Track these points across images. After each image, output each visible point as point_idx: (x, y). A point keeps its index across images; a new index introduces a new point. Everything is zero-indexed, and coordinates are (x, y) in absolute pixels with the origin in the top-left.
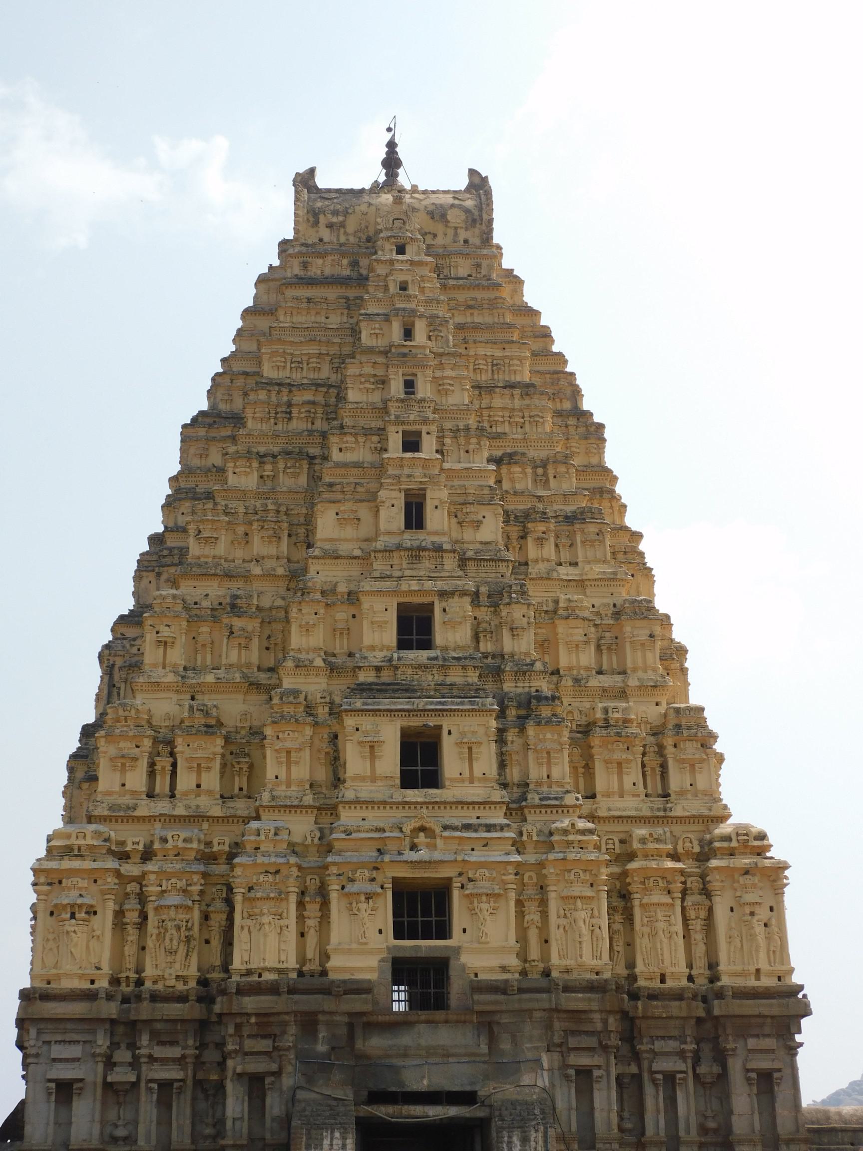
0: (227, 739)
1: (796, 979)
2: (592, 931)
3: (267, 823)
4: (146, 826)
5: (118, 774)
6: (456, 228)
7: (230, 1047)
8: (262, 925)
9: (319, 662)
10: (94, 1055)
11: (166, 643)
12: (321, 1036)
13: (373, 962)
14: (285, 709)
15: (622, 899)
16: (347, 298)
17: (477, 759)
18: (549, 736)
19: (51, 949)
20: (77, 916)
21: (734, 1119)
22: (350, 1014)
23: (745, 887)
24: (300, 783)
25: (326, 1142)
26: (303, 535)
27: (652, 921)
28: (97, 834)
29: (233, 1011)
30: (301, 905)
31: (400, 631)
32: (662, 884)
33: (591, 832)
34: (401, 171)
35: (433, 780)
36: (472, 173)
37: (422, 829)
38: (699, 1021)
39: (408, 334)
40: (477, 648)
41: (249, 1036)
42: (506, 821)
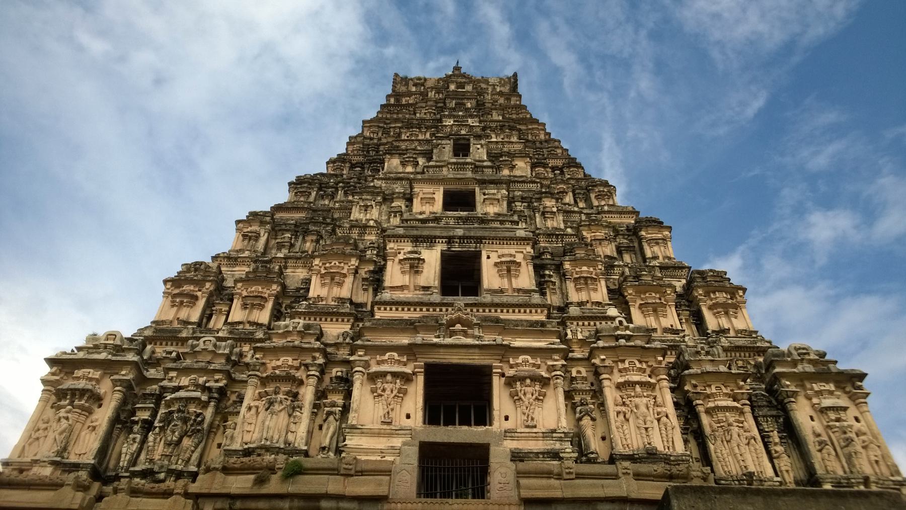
6: (494, 85)
8: (271, 403)
13: (397, 442)
17: (517, 276)
18: (585, 268)
19: (38, 439)
20: (76, 402)
24: (341, 301)
29: (213, 491)
30: (321, 395)
37: (459, 321)
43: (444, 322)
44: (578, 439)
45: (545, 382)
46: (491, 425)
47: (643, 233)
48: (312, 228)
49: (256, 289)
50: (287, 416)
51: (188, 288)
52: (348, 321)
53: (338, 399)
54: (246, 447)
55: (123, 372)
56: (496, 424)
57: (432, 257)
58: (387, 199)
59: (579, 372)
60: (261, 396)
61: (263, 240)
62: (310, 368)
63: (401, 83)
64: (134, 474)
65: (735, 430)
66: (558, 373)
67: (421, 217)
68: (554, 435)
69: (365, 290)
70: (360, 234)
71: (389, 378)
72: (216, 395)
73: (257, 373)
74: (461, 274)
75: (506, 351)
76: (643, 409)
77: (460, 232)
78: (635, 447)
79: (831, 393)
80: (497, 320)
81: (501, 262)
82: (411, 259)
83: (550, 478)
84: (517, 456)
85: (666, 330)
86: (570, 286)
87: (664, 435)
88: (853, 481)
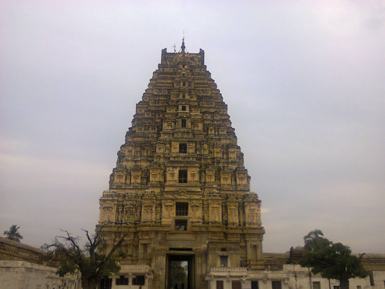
0: (142, 172)
1: (262, 226)
3: (149, 190)
4: (125, 190)
6: (196, 62)
7: (140, 238)
8: (147, 212)
9: (162, 156)
10: (111, 239)
13: (171, 220)
14: (154, 166)
15: (225, 207)
16: (172, 77)
17: (195, 177)
18: (210, 172)
21: (248, 255)
22: (166, 231)
23: (252, 205)
24: (157, 182)
25: (159, 259)
26: (160, 128)
27: (232, 212)
28: (114, 192)
30: (156, 208)
31: (180, 150)
32: (234, 204)
33: (218, 193)
34: (185, 49)
35: (185, 181)
36: (201, 49)
37: (182, 192)
38: (241, 234)
39: (184, 85)
40: (196, 153)
41: (144, 236)
42: (200, 191)
44: (203, 219)
47: (229, 149)
48: (146, 148)
51: (120, 173)
53: (159, 209)
57: (176, 171)
58: (164, 143)
60: (145, 210)
61: (133, 151)
63: (164, 60)
65: (233, 214)
69: (162, 178)
71: (169, 206)
74: (183, 175)
75: (191, 200)
76: (216, 213)
77: (183, 165)
84: (192, 222)
86: (207, 176)
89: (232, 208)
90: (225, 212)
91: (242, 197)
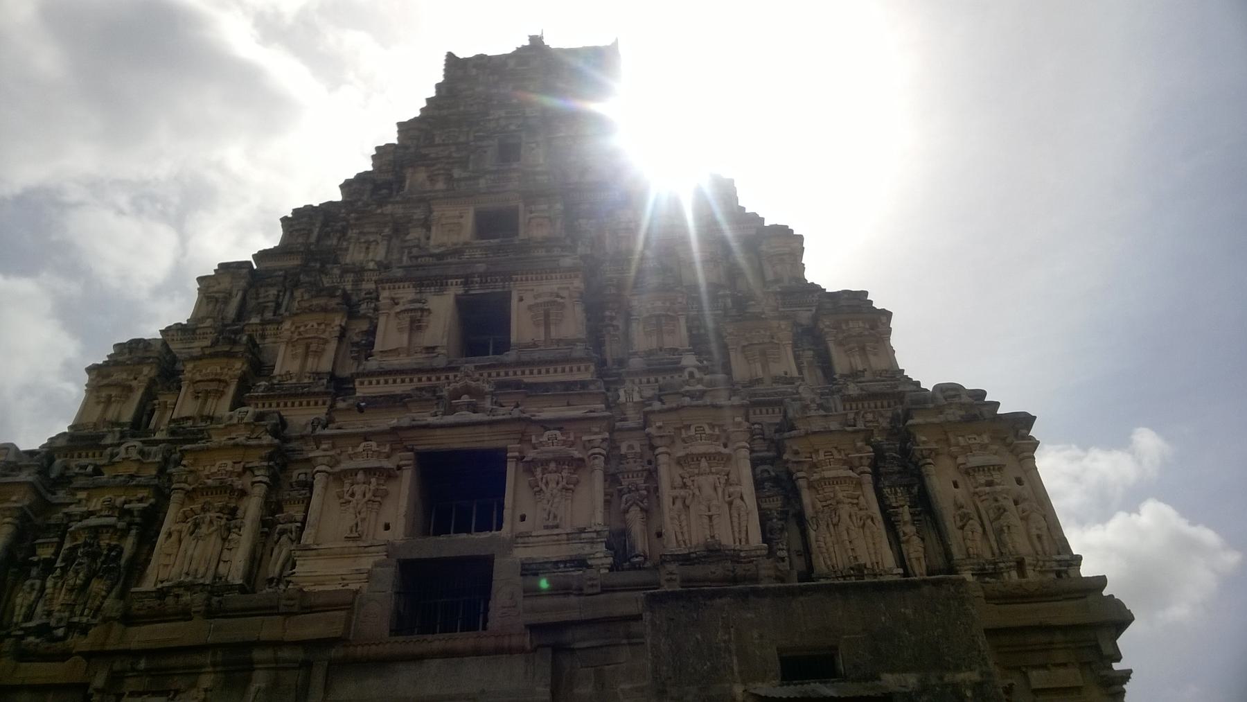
2: (730, 504)
5: (101, 406)
8: (197, 525)
11: (217, 300)
12: (253, 688)
13: (366, 563)
24: (318, 375)
30: (272, 508)
37: (468, 390)
41: (132, 694)
43: (445, 393)
45: (578, 464)
46: (499, 528)
49: (213, 368)
50: (219, 541)
52: (324, 403)
54: (159, 586)
55: (14, 498)
56: (506, 526)
59: (631, 447)
62: (257, 473)
64: (29, 632)
65: (845, 510)
66: (597, 450)
67: (437, 251)
68: (583, 535)
70: (357, 282)
71: (360, 476)
72: (138, 520)
73: (182, 485)
76: (707, 490)
78: (694, 543)
79: (984, 447)
80: (518, 385)
81: (537, 305)
82: (412, 310)
83: (568, 594)
85: (776, 380)
87: (736, 524)
88: (1002, 565)
89: (828, 474)
90: (784, 515)
91: (884, 423)
